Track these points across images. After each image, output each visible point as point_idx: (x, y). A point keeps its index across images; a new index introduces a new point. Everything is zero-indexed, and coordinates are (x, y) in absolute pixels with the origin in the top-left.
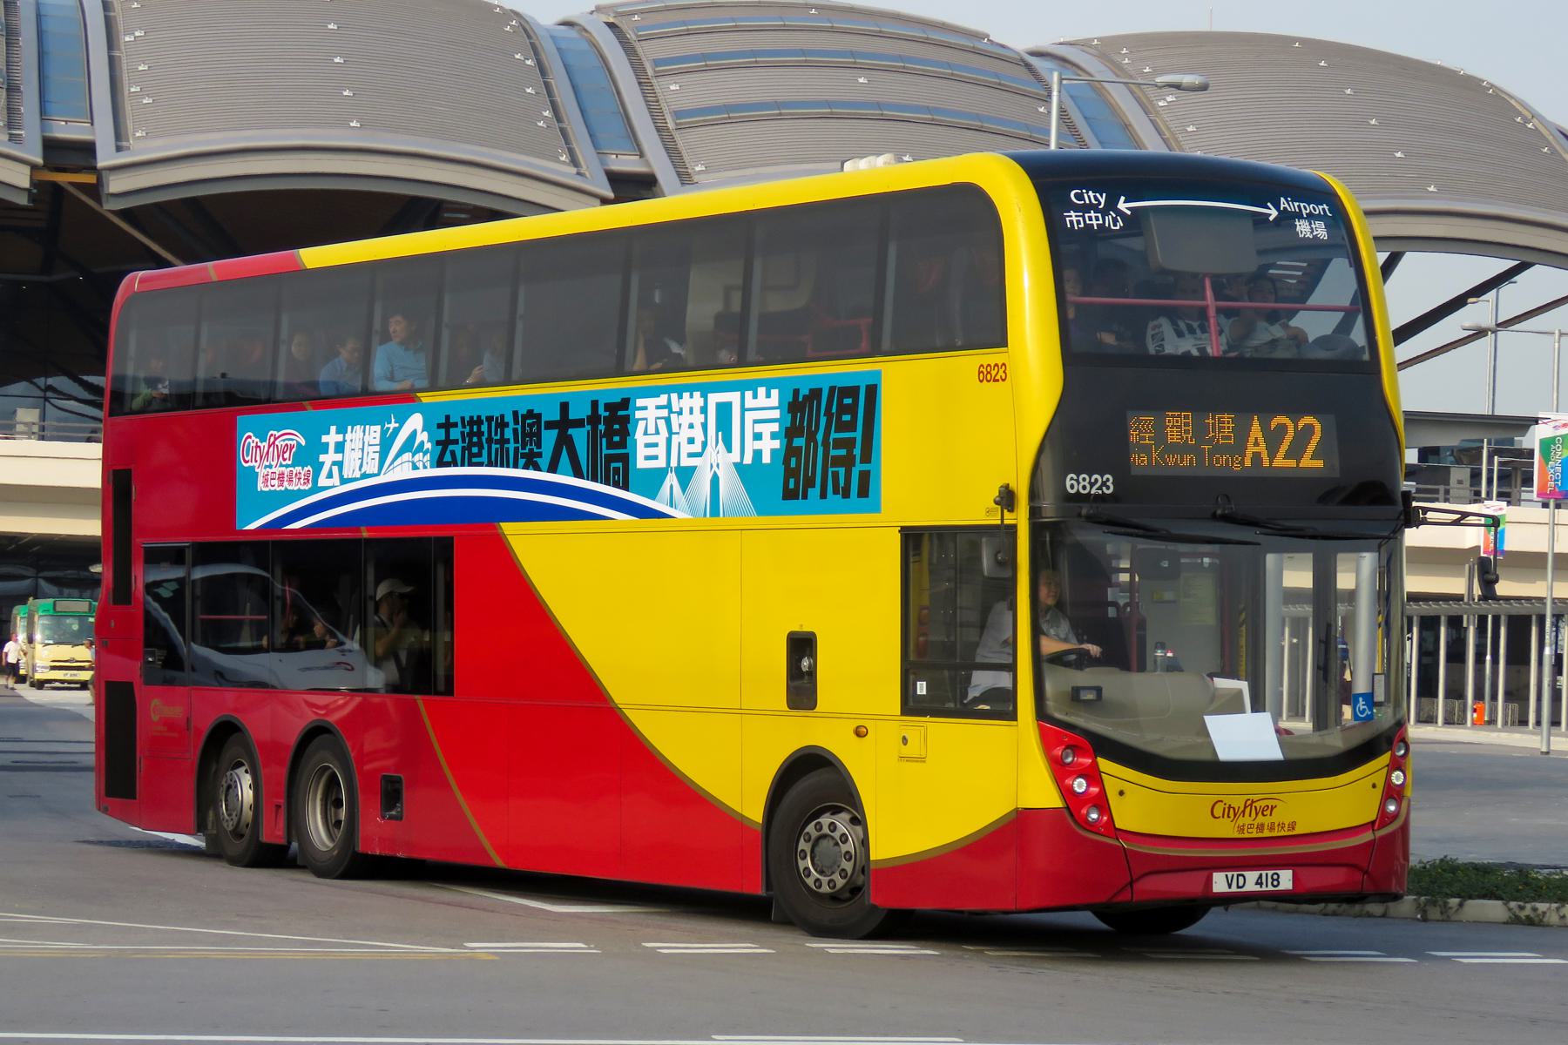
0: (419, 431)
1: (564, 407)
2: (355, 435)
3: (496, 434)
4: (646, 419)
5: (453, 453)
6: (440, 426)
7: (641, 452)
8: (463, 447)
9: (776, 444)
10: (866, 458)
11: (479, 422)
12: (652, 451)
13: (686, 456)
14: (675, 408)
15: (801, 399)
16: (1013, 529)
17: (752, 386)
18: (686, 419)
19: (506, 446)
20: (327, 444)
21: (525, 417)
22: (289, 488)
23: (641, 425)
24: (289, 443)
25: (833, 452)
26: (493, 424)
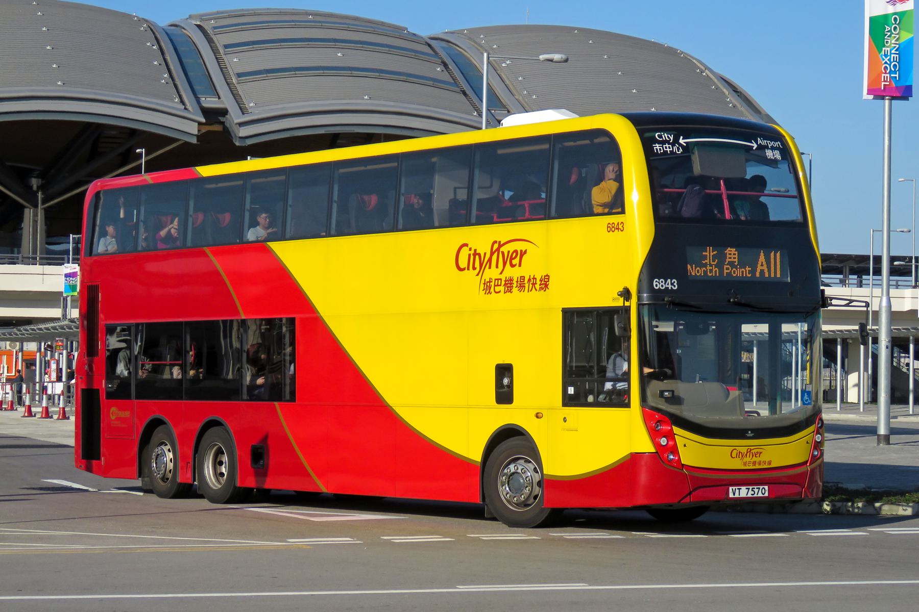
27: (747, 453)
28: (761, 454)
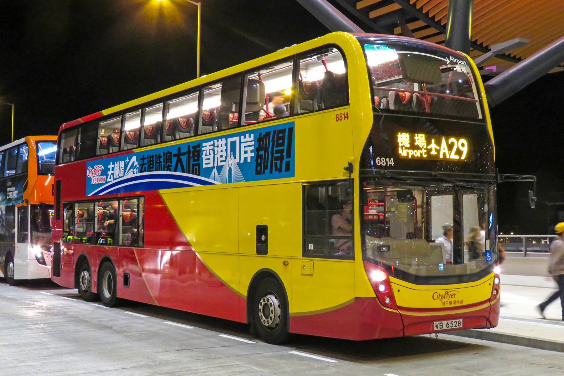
0: (135, 161)
1: (179, 149)
2: (117, 164)
3: (158, 160)
4: (206, 150)
5: (145, 168)
6: (141, 159)
7: (204, 162)
8: (148, 166)
9: (253, 154)
10: (289, 156)
11: (153, 157)
12: (208, 161)
13: (220, 162)
14: (216, 145)
15: (262, 136)
16: (353, 179)
17: (244, 134)
18: (220, 149)
19: (161, 164)
20: (110, 168)
21: (167, 154)
22: (100, 183)
23: (204, 152)
24: (99, 169)
25: (275, 155)
26: (157, 157)
27: (445, 295)
28: (456, 295)
